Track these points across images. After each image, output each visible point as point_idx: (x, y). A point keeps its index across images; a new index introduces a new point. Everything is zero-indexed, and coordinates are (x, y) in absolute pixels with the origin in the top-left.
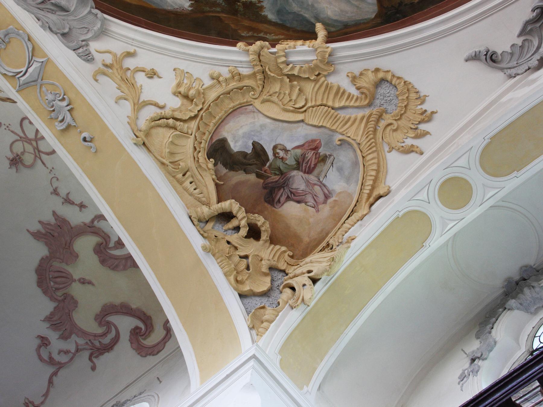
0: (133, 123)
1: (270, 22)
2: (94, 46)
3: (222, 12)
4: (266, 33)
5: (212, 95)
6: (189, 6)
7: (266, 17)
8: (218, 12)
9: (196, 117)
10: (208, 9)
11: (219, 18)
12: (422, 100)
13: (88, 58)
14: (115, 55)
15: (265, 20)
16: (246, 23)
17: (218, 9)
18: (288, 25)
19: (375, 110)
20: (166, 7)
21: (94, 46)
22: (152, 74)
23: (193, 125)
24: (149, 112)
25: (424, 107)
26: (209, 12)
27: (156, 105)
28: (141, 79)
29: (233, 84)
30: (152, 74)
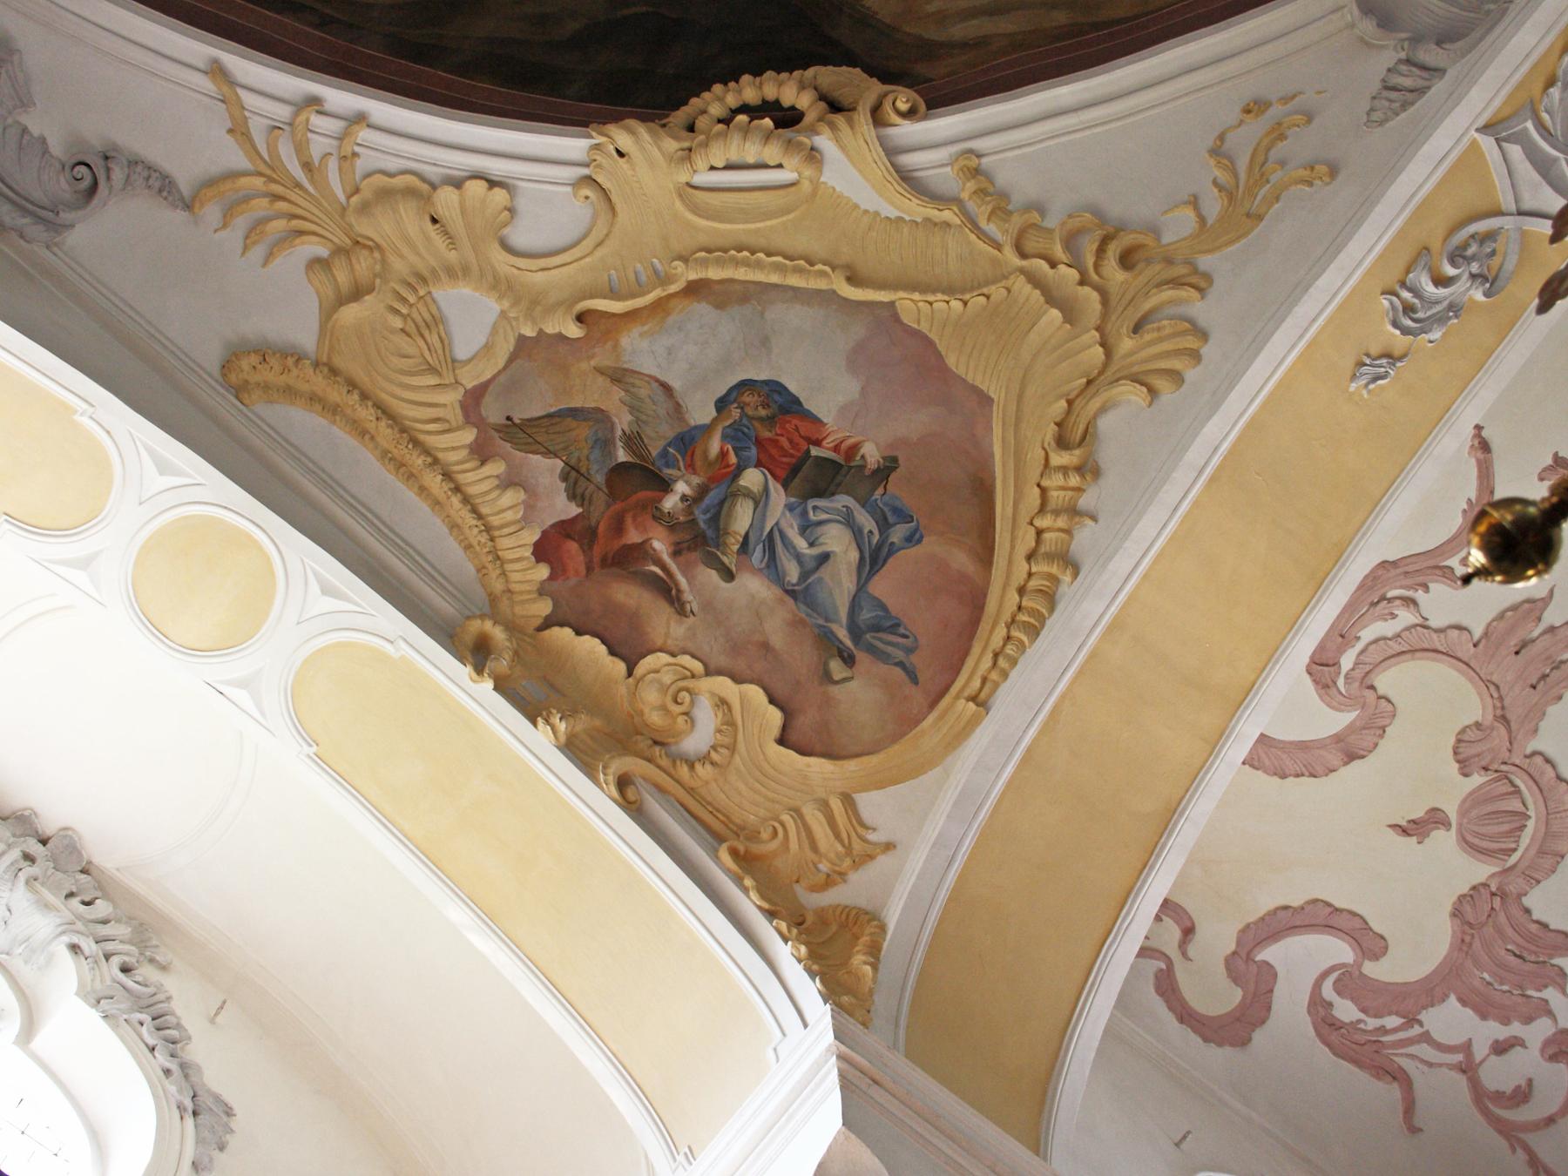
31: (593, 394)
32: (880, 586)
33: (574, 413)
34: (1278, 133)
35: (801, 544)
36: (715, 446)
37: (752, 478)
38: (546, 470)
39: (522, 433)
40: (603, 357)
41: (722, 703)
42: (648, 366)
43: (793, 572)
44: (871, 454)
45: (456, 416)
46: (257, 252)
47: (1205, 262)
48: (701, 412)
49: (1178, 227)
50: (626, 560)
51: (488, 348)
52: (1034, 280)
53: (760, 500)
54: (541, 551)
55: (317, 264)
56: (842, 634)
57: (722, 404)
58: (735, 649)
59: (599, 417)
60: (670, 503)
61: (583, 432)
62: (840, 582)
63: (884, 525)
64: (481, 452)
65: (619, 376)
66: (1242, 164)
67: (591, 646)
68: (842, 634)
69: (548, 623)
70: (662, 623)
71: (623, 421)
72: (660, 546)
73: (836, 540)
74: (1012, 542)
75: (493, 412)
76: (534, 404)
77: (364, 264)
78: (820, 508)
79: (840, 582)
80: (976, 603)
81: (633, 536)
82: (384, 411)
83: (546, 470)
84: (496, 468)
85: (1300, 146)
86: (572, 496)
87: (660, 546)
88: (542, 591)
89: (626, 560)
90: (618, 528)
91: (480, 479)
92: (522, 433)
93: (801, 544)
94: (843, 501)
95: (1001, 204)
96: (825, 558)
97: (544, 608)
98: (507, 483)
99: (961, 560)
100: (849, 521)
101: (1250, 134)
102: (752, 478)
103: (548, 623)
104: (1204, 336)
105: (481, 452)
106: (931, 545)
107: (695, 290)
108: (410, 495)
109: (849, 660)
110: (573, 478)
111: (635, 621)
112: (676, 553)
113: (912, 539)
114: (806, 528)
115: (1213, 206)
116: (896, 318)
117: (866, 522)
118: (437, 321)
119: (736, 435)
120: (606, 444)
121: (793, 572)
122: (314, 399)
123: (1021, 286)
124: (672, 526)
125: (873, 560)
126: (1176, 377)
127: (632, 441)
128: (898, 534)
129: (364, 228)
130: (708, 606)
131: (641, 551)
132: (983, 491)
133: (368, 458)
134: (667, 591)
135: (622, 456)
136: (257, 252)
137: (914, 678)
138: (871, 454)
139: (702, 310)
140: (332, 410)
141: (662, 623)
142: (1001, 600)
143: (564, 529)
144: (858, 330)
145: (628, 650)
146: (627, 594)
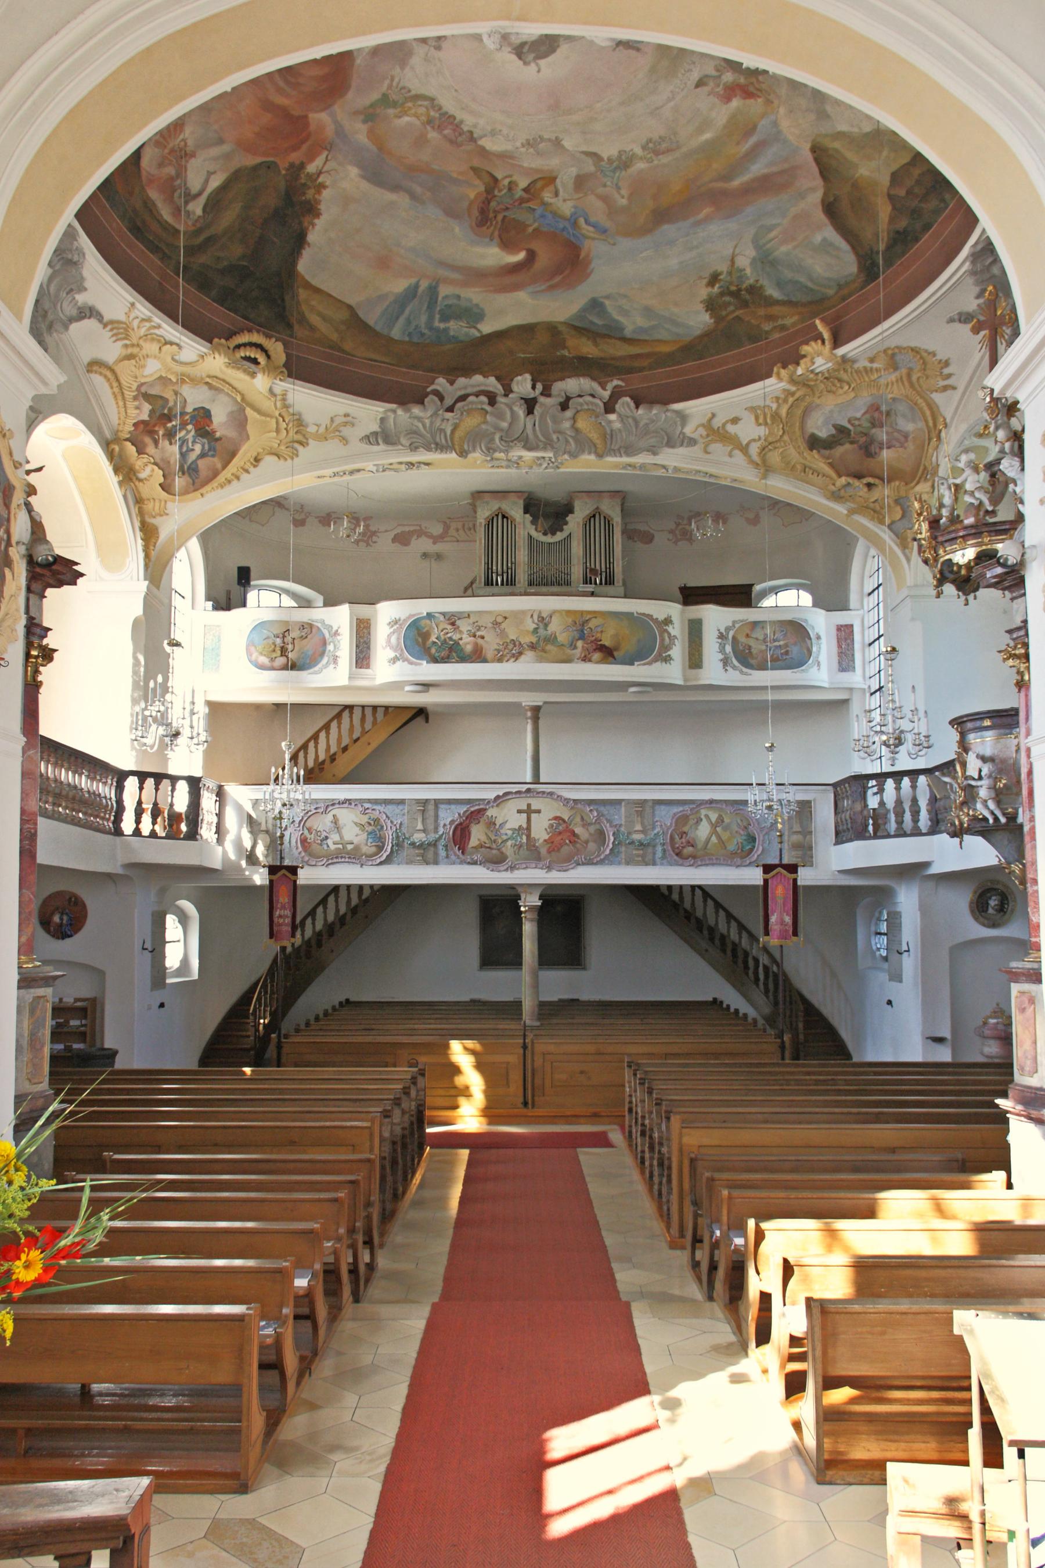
0: (752, 462)
1: (777, 302)
2: (688, 430)
3: (737, 309)
4: (783, 317)
5: (783, 412)
6: (711, 318)
7: (771, 297)
8: (733, 311)
9: (784, 432)
10: (724, 313)
11: (738, 319)
12: (934, 354)
13: (692, 442)
14: (703, 425)
15: (770, 302)
16: (761, 312)
17: (732, 308)
18: (794, 299)
19: (904, 371)
20: (698, 332)
21: (688, 430)
22: (735, 421)
23: (786, 438)
24: (754, 450)
25: (938, 357)
26: (727, 315)
27: (754, 440)
28: (731, 428)
29: (791, 400)
30: (735, 421)
31: (168, 395)
32: (200, 463)
33: (161, 397)
34: (345, 424)
35: (190, 444)
36: (187, 417)
37: (190, 427)
38: (147, 407)
39: (147, 397)
40: (175, 388)
41: (153, 470)
42: (184, 394)
43: (185, 449)
44: (218, 435)
45: (134, 387)
46: (114, 338)
47: (311, 441)
48: (189, 409)
49: (312, 429)
50: (152, 433)
51: (152, 375)
52: (277, 423)
53: (188, 432)
54: (135, 425)
55: (126, 346)
56: (186, 467)
57: (195, 410)
58: (162, 460)
59: (167, 401)
60: (169, 425)
61: (160, 402)
62: (192, 457)
63: (210, 450)
64: (135, 398)
65: (176, 393)
66: (334, 425)
67: (134, 449)
68: (186, 467)
69: (127, 440)
70: (151, 449)
71: (171, 404)
72: (161, 433)
73: (198, 448)
74: (232, 467)
75: (143, 390)
76: (153, 392)
77: (135, 350)
78: (199, 440)
79: (192, 457)
80: (215, 474)
81: (157, 429)
82: (120, 384)
83: (147, 407)
84: (136, 403)
85: (346, 431)
86: (150, 416)
87: (161, 433)
88: (130, 432)
89: (152, 433)
90: (154, 426)
91: (131, 405)
92: (147, 397)
93: (190, 444)
94: (205, 441)
95: (284, 400)
96: (193, 450)
97: (128, 436)
98: (137, 408)
99: (219, 466)
100: (203, 446)
101: (339, 420)
102: (190, 427)
103: (127, 440)
104: (297, 456)
105: (135, 398)
106: (216, 460)
107: (207, 383)
108: (115, 406)
109: (183, 473)
110: (152, 412)
111: (145, 445)
112: (163, 435)
113: (213, 456)
114: (194, 442)
115: (322, 430)
116: (244, 410)
117: (207, 447)
118: (144, 366)
119: (193, 417)
120: (164, 408)
121: (185, 449)
122: (105, 377)
123: (274, 421)
124: (166, 429)
125: (203, 455)
126: (286, 459)
127: (170, 409)
128: (211, 453)
129: (141, 342)
130: (163, 448)
131: (157, 432)
132: (233, 454)
133: (109, 391)
134: (156, 443)
135: (166, 411)
136: (114, 338)
137: (194, 484)
138: (218, 435)
139: (206, 388)
140: (108, 380)
141: (151, 449)
142: (221, 478)
143: (143, 422)
144: (235, 408)
145: (140, 452)
146: (148, 440)
